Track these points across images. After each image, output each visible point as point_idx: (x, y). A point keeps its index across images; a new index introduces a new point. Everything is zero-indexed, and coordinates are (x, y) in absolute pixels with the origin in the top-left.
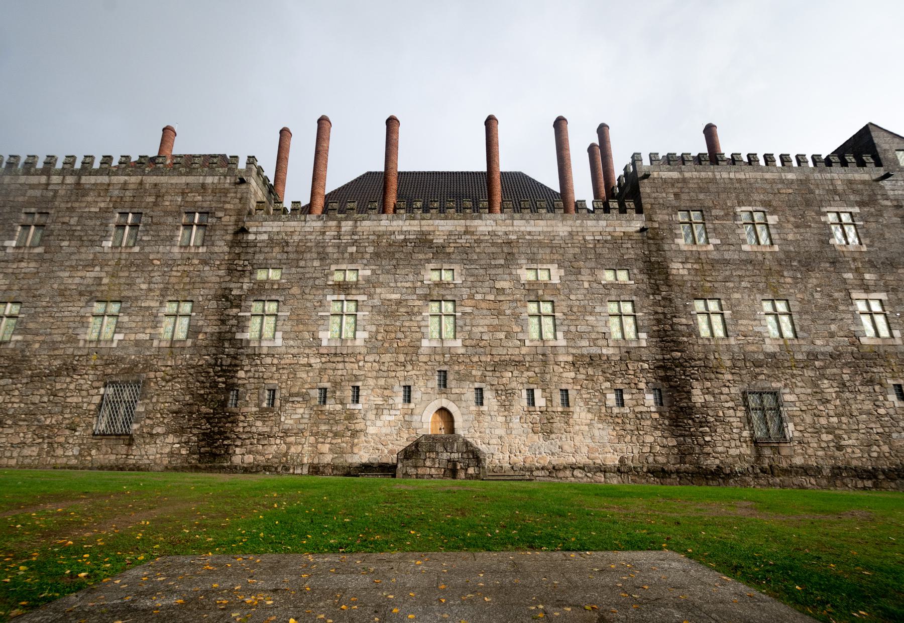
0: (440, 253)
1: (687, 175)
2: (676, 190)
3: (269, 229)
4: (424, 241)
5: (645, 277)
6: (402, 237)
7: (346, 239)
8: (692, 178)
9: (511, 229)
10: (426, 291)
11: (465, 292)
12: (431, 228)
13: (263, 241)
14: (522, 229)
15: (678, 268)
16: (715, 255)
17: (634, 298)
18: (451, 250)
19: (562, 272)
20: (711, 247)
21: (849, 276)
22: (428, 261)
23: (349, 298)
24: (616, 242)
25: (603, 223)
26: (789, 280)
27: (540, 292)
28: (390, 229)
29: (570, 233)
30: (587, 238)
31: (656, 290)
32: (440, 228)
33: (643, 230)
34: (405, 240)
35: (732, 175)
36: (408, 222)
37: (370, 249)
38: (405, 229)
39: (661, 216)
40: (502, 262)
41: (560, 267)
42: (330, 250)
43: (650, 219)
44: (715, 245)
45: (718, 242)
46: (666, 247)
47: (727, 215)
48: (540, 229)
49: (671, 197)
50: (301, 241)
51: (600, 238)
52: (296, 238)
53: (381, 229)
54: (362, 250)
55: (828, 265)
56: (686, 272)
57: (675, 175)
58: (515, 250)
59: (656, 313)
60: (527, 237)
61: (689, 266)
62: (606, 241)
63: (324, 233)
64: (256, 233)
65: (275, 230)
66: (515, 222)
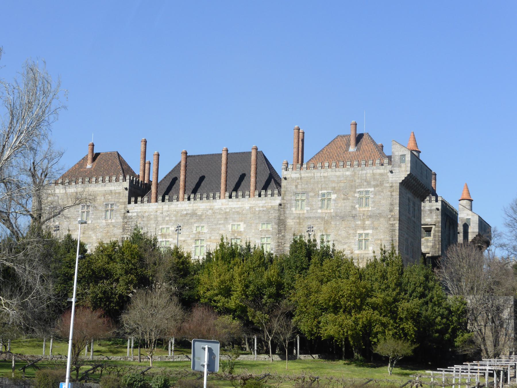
0: (200, 218)
1: (303, 175)
2: (297, 184)
3: (137, 211)
4: (193, 214)
5: (276, 226)
6: (186, 212)
7: (165, 214)
8: (304, 177)
9: (227, 206)
10: (194, 236)
11: (208, 236)
12: (197, 208)
13: (134, 216)
14: (232, 206)
15: (290, 222)
16: (306, 215)
17: (271, 236)
18: (204, 217)
19: (245, 225)
20: (305, 212)
21: (359, 222)
22: (195, 223)
23: (166, 240)
24: (267, 211)
25: (264, 202)
26: (333, 226)
27: (236, 235)
28: (182, 208)
29: (250, 207)
30: (257, 209)
31: (280, 232)
32: (201, 207)
33: (280, 205)
34: (187, 214)
35: (322, 175)
36: (188, 205)
37: (174, 219)
38: (187, 208)
39: (288, 197)
40: (222, 222)
41: (245, 223)
42: (159, 219)
43: (283, 199)
44: (307, 211)
45: (309, 209)
46: (287, 212)
47: (315, 195)
48: (238, 206)
49: (294, 187)
50: (149, 215)
51: (261, 209)
52: (147, 214)
53: (178, 208)
54: (171, 218)
55: (351, 218)
56: (293, 223)
57: (298, 175)
58: (228, 217)
59: (278, 242)
60: (233, 210)
61: (295, 221)
62: (263, 210)
63: (157, 211)
64: (132, 213)
65: (139, 211)
66: (230, 203)
